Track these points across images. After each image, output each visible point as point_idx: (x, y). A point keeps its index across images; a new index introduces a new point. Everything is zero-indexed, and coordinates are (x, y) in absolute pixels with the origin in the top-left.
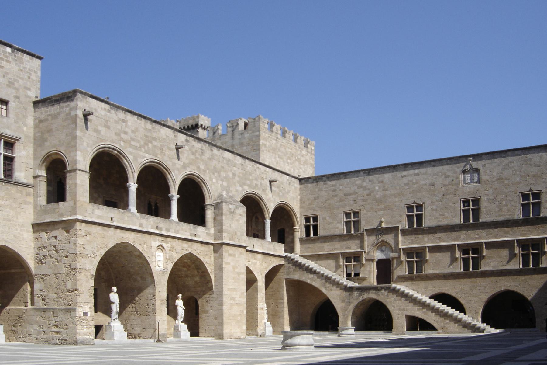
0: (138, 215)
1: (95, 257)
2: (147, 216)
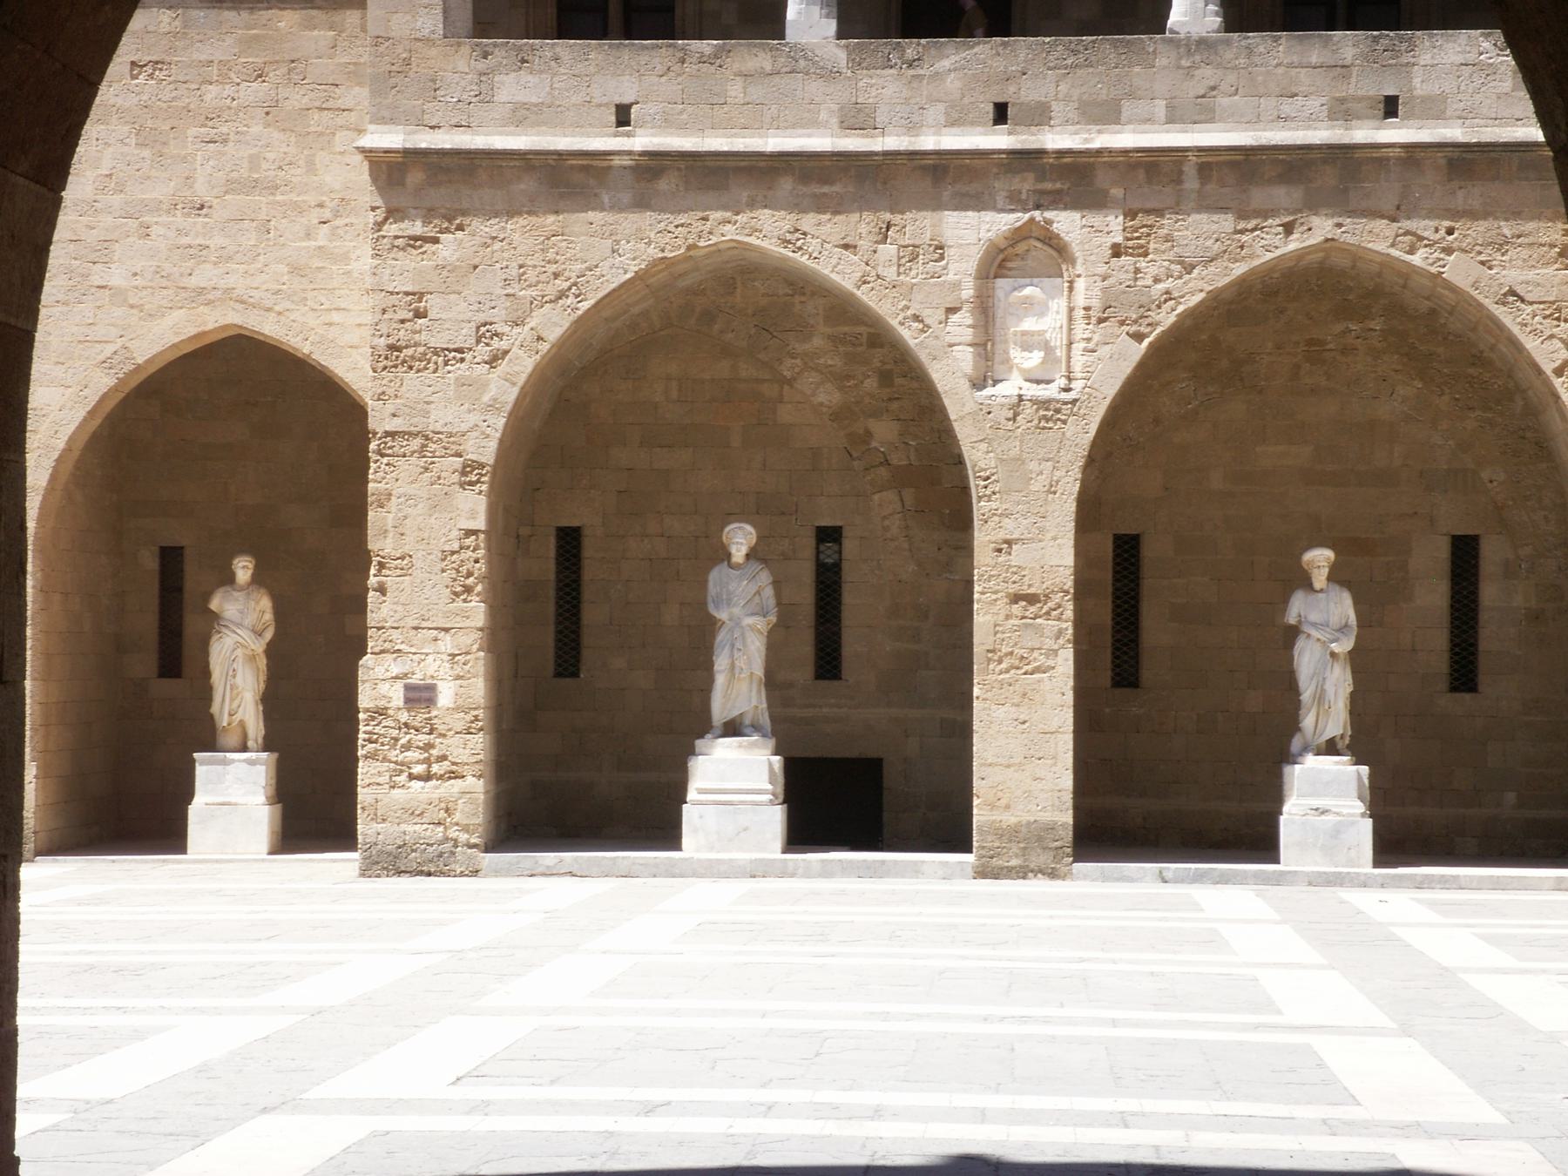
0: (837, 53)
1: (493, 361)
2: (912, 47)
